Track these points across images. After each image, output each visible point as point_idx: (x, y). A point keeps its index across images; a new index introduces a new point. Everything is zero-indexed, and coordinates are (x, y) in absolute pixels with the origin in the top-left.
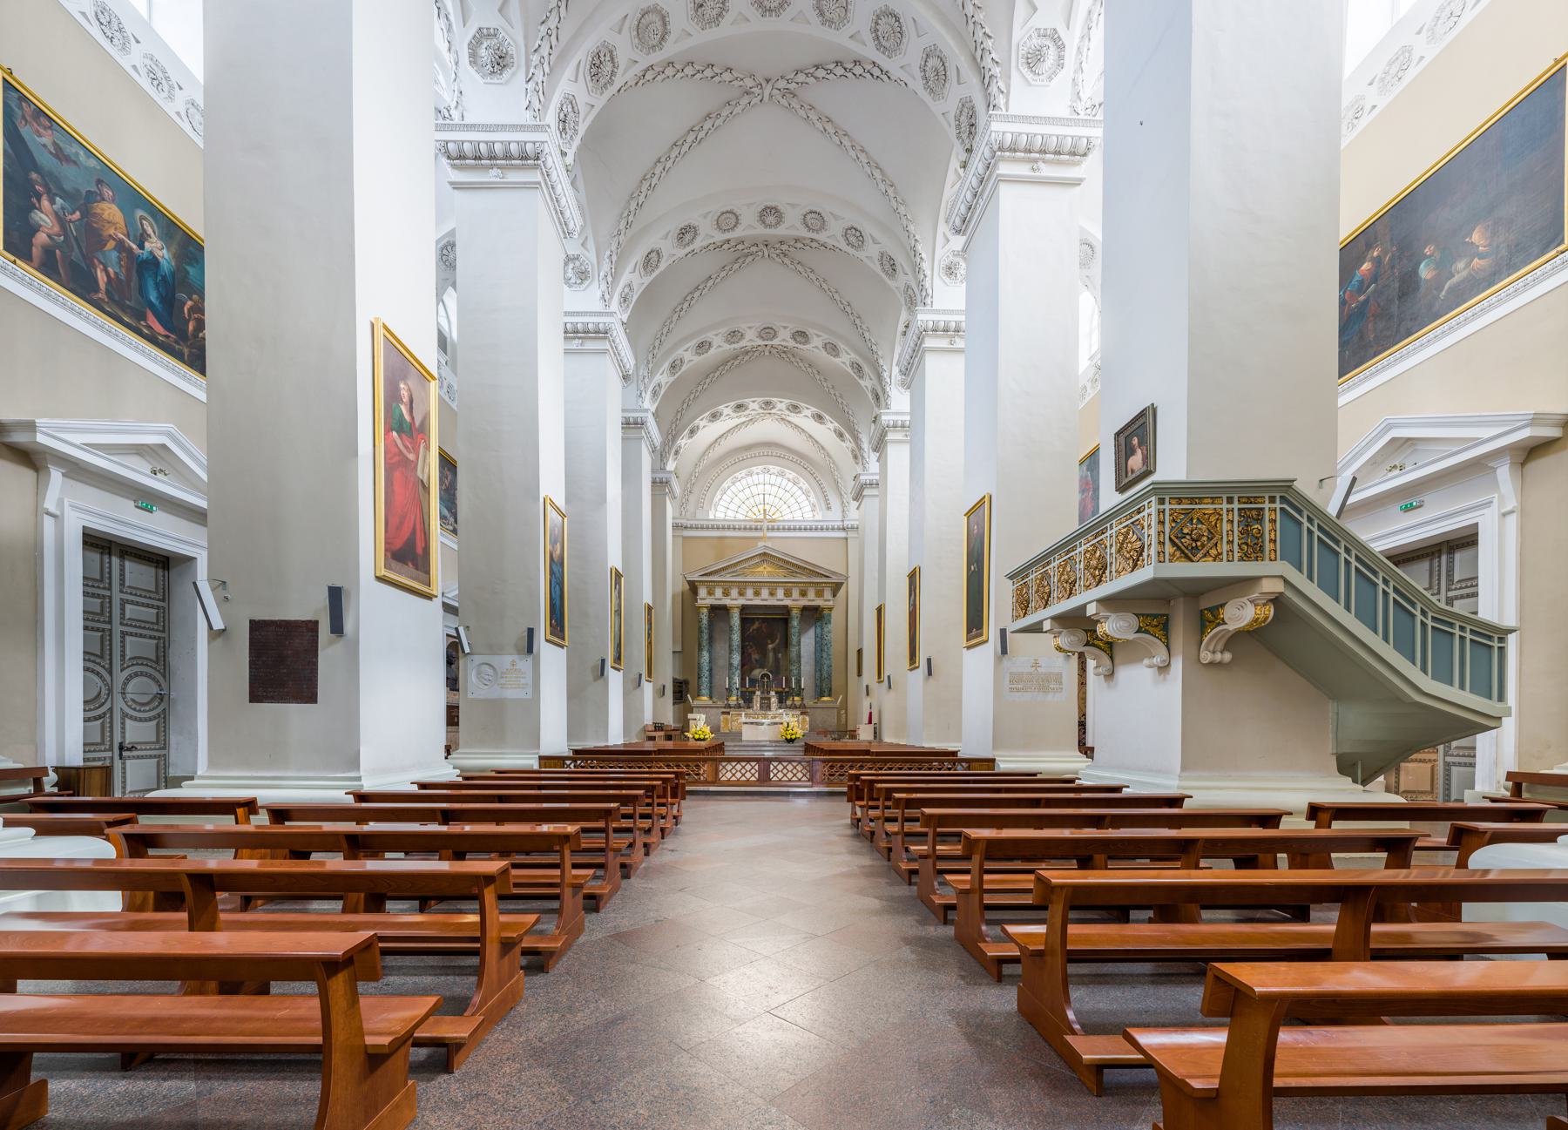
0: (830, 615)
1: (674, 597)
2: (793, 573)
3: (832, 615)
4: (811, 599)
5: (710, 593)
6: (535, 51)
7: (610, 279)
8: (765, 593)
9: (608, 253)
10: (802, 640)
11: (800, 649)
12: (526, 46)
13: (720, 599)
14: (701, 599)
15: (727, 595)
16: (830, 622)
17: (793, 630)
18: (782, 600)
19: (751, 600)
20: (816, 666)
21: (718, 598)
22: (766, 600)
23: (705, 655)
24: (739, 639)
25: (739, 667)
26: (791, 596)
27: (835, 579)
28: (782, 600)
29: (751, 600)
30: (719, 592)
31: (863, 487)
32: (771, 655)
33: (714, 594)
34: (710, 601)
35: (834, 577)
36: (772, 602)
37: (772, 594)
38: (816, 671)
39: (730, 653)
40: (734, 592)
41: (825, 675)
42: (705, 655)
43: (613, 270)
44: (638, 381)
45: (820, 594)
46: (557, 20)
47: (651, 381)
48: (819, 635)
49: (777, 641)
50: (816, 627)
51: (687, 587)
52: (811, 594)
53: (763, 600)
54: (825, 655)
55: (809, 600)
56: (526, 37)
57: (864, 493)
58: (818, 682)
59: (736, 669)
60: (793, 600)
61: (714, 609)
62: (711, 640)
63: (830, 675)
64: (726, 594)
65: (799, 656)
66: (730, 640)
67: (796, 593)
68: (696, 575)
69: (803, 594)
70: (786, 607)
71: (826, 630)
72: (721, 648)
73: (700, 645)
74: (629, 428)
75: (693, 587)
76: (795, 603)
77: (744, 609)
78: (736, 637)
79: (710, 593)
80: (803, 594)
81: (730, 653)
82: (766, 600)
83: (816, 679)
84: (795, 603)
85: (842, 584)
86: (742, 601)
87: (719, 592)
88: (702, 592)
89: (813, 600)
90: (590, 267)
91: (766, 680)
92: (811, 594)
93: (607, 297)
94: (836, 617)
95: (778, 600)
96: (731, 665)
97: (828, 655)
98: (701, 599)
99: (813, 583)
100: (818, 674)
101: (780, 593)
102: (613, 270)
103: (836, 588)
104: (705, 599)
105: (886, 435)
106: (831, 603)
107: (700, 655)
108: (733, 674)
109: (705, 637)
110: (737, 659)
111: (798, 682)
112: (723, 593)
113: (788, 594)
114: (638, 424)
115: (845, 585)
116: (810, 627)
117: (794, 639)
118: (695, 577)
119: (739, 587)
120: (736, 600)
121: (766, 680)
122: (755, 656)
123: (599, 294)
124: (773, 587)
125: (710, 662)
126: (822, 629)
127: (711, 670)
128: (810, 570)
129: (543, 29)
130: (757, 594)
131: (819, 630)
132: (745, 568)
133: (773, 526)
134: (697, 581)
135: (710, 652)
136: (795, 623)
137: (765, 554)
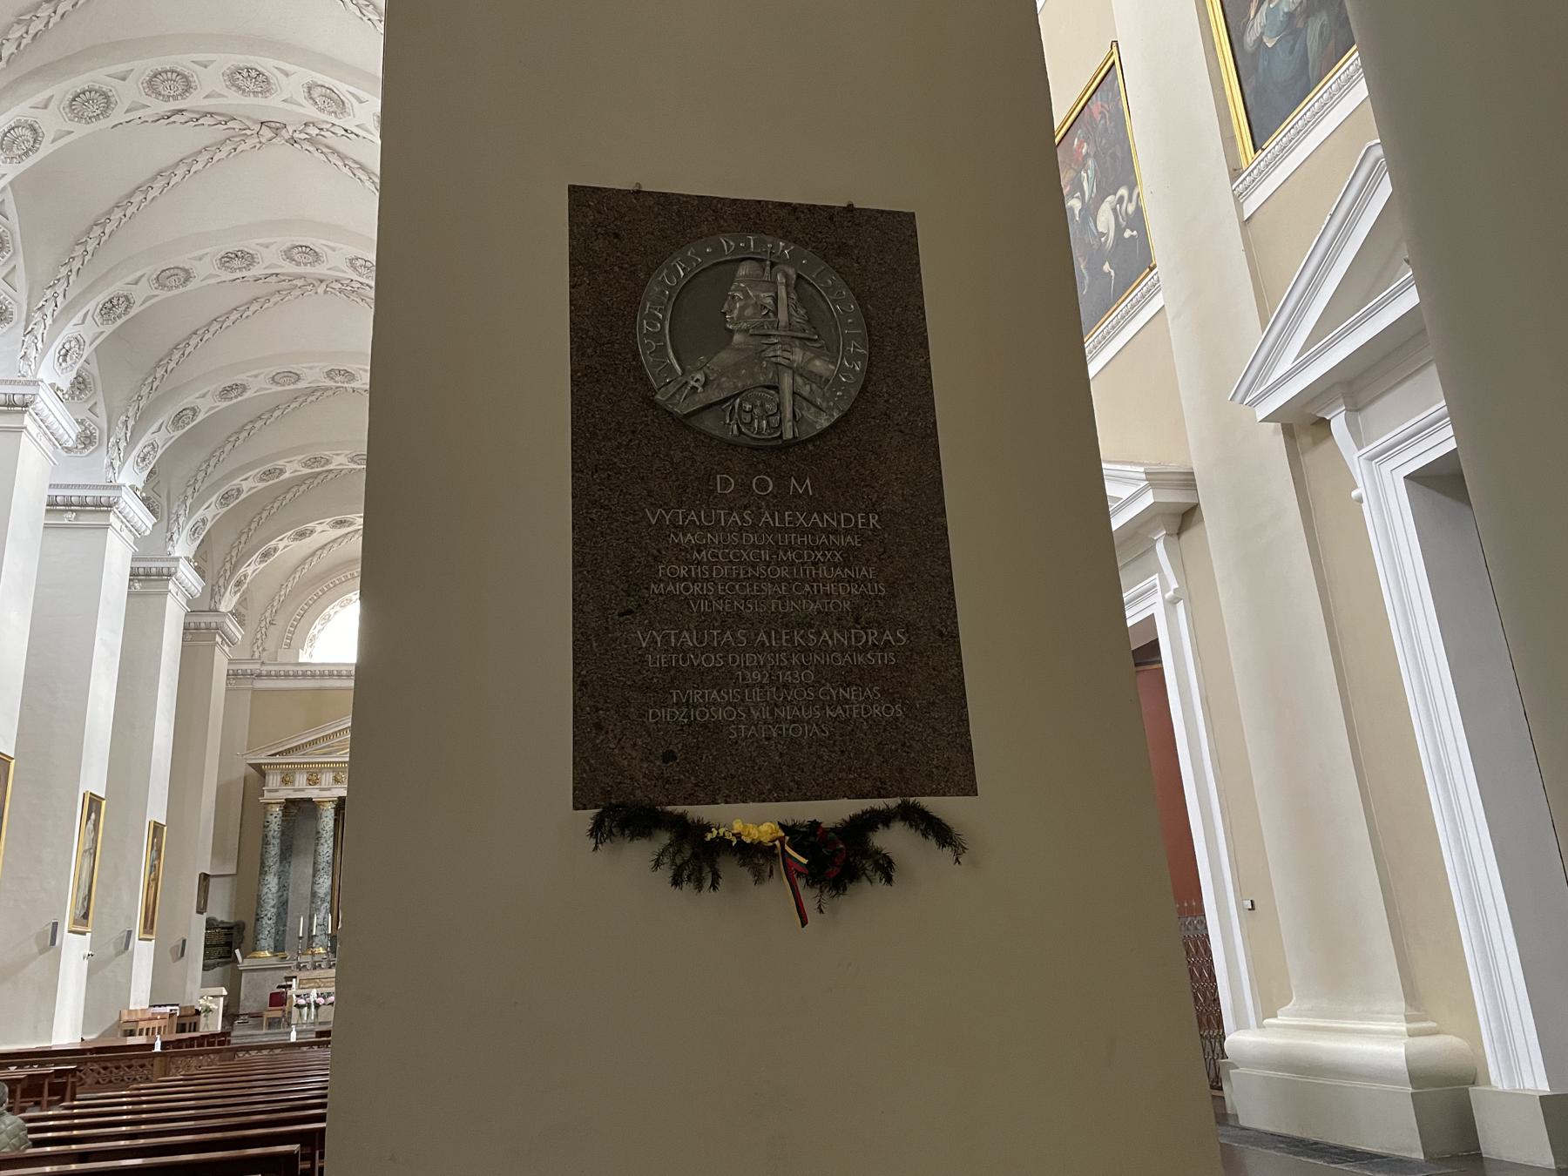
1: (222, 792)
6: (39, 309)
7: (123, 444)
9: (123, 418)
12: (28, 304)
13: (302, 790)
14: (269, 791)
15: (315, 783)
21: (301, 788)
23: (272, 882)
33: (293, 783)
42: (272, 882)
43: (128, 435)
44: (169, 521)
46: (66, 284)
47: (188, 519)
56: (29, 297)
59: (323, 901)
61: (289, 804)
62: (286, 853)
64: (313, 781)
72: (301, 869)
73: (263, 864)
87: (301, 780)
88: (273, 780)
90: (98, 432)
93: (117, 464)
96: (314, 894)
98: (269, 791)
102: (128, 435)
104: (277, 791)
109: (274, 850)
110: (325, 883)
112: (308, 780)
119: (334, 770)
120: (329, 789)
123: (106, 461)
129: (49, 293)
134: (265, 764)
135: (281, 875)
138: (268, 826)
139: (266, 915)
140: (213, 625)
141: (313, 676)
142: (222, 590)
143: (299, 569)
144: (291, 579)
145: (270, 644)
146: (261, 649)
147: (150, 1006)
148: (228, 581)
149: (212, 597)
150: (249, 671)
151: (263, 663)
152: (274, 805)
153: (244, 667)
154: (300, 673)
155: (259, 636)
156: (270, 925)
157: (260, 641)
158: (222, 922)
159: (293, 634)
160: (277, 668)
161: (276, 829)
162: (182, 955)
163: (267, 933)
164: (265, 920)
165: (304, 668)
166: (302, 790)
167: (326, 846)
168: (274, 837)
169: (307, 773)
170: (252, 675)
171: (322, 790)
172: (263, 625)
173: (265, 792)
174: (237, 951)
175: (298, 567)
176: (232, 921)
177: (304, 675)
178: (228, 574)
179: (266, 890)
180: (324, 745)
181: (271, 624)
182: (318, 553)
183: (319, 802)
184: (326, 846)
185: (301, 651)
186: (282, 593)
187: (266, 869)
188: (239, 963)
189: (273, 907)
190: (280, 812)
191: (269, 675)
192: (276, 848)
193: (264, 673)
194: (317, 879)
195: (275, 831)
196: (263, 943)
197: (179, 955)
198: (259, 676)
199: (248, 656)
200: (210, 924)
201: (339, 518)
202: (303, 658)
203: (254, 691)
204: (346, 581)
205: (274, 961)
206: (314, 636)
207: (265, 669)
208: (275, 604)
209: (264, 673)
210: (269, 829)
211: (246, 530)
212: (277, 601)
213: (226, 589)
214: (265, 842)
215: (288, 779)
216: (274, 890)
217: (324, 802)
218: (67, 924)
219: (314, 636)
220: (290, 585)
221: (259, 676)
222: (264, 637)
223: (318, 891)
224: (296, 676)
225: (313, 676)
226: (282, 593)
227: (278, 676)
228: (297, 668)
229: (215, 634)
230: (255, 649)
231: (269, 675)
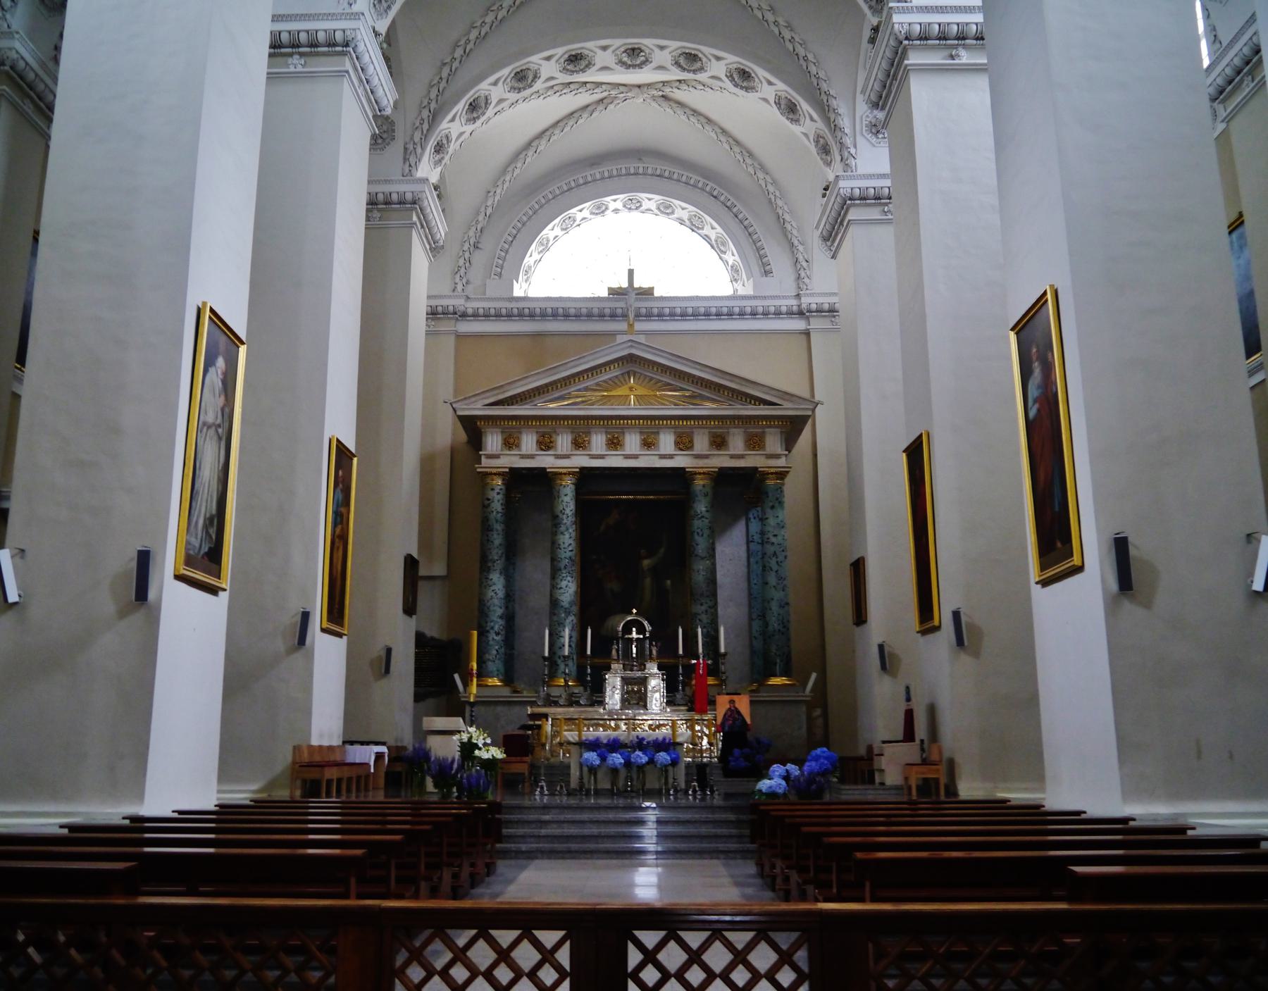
0: (780, 489)
2: (693, 399)
3: (785, 488)
4: (736, 455)
5: (510, 443)
8: (632, 442)
10: (719, 548)
11: (714, 564)
13: (532, 457)
15: (549, 448)
16: (781, 503)
17: (697, 523)
18: (671, 457)
19: (602, 457)
20: (750, 606)
22: (635, 457)
24: (574, 544)
25: (575, 609)
26: (690, 447)
27: (788, 410)
28: (671, 457)
29: (602, 457)
30: (529, 442)
31: (847, 202)
32: (648, 581)
33: (518, 446)
34: (511, 461)
35: (787, 405)
36: (648, 461)
37: (648, 444)
38: (751, 619)
39: (553, 577)
40: (563, 442)
41: (774, 624)
45: (755, 442)
48: (757, 538)
49: (662, 550)
50: (748, 520)
51: (463, 436)
52: (737, 442)
53: (627, 457)
54: (772, 580)
55: (732, 457)
57: (850, 217)
58: (758, 644)
59: (568, 613)
60: (698, 457)
62: (512, 552)
63: (785, 624)
64: (545, 444)
65: (712, 581)
66: (554, 545)
67: (701, 442)
68: (479, 406)
69: (719, 442)
70: (679, 473)
71: (772, 521)
72: (534, 570)
74: (318, 54)
75: (473, 428)
76: (701, 463)
77: (586, 477)
78: (568, 540)
79: (510, 443)
80: (719, 442)
81: (553, 577)
82: (635, 457)
83: (751, 637)
84: (701, 463)
85: (808, 417)
86: (581, 461)
87: (529, 442)
88: (493, 442)
89: (741, 457)
91: (634, 635)
92: (737, 442)
94: (794, 490)
95: (663, 457)
96: (554, 603)
97: (780, 578)
99: (739, 417)
100: (757, 625)
101: (667, 442)
103: (793, 427)
105: (904, 55)
106: (782, 462)
107: (483, 582)
108: (562, 624)
109: (497, 539)
110: (568, 588)
111: (712, 640)
113: (684, 443)
114: (335, 45)
115: (810, 422)
116: (736, 519)
117: (701, 544)
118: (477, 409)
121: (634, 635)
122: (613, 586)
124: (649, 428)
125: (509, 597)
126: (763, 520)
127: (509, 618)
128: (733, 390)
130: (614, 443)
131: (755, 527)
132: (586, 389)
133: (649, 310)
136: (701, 507)
137: (631, 359)
138: (489, 505)
139: (492, 628)
140: (409, 197)
141: (532, 315)
142: (419, 150)
143: (510, 169)
144: (500, 183)
145: (476, 274)
146: (464, 281)
147: (344, 742)
148: (426, 137)
149: (405, 160)
150: (451, 309)
151: (468, 298)
152: (495, 477)
153: (445, 302)
154: (515, 311)
155: (461, 262)
156: (498, 642)
157: (463, 270)
158: (432, 639)
159: (510, 246)
160: (486, 305)
161: (499, 509)
162: (387, 671)
163: (495, 652)
164: (492, 636)
165: (521, 305)
166: (532, 457)
167: (567, 536)
168: (497, 521)
169: (537, 432)
170: (455, 313)
171: (558, 457)
172: (466, 248)
173: (483, 459)
174: (456, 676)
175: (508, 166)
176: (444, 637)
177: (521, 315)
178: (426, 126)
179: (491, 594)
180: (557, 395)
181: (476, 247)
182: (534, 144)
183: (556, 474)
184: (567, 536)
185: (515, 282)
186: (489, 203)
187: (490, 564)
188: (460, 693)
189: (501, 617)
190: (503, 487)
191: (475, 315)
192: (501, 536)
193: (470, 311)
194: (558, 581)
195: (498, 512)
196: (492, 666)
197: (383, 671)
198: (464, 315)
199: (447, 292)
200: (421, 639)
201: (575, 47)
202: (518, 291)
203: (460, 337)
204: (568, 190)
205: (506, 692)
206: (530, 267)
207: (471, 306)
208: (481, 218)
209: (470, 311)
210: (489, 510)
211: (448, 60)
212: (483, 214)
213: (423, 149)
214: (486, 527)
215: (512, 440)
216: (501, 594)
217: (561, 474)
218: (169, 560)
219: (530, 267)
220: (498, 191)
221: (464, 315)
222: (467, 264)
223: (559, 598)
224: (510, 316)
225: (532, 315)
226: (489, 203)
227: (487, 316)
228: (509, 305)
229: (412, 210)
230: (457, 280)
231: (475, 315)
